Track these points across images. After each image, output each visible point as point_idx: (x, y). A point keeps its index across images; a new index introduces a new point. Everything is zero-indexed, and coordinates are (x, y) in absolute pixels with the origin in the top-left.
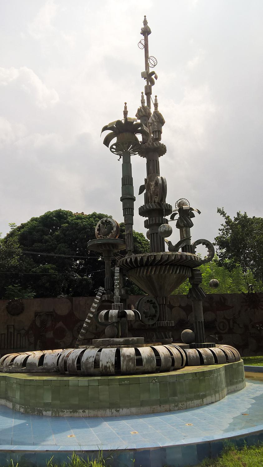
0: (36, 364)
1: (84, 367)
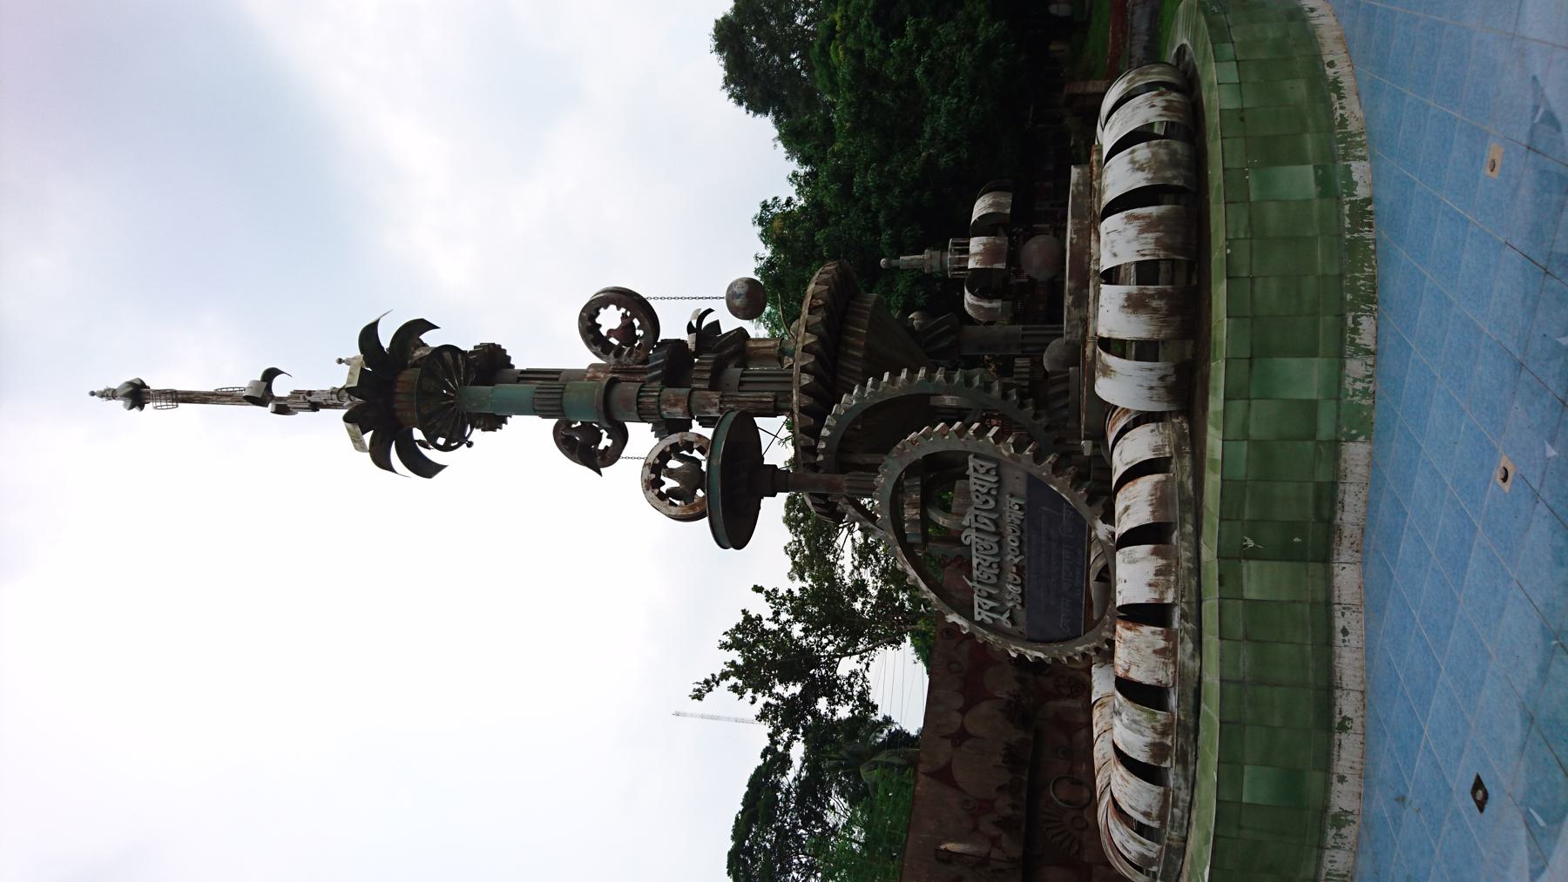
0: (1158, 482)
1: (1169, 174)
